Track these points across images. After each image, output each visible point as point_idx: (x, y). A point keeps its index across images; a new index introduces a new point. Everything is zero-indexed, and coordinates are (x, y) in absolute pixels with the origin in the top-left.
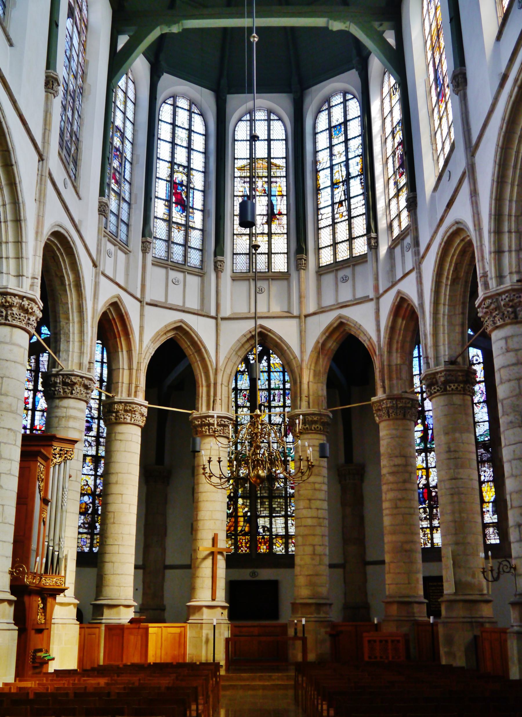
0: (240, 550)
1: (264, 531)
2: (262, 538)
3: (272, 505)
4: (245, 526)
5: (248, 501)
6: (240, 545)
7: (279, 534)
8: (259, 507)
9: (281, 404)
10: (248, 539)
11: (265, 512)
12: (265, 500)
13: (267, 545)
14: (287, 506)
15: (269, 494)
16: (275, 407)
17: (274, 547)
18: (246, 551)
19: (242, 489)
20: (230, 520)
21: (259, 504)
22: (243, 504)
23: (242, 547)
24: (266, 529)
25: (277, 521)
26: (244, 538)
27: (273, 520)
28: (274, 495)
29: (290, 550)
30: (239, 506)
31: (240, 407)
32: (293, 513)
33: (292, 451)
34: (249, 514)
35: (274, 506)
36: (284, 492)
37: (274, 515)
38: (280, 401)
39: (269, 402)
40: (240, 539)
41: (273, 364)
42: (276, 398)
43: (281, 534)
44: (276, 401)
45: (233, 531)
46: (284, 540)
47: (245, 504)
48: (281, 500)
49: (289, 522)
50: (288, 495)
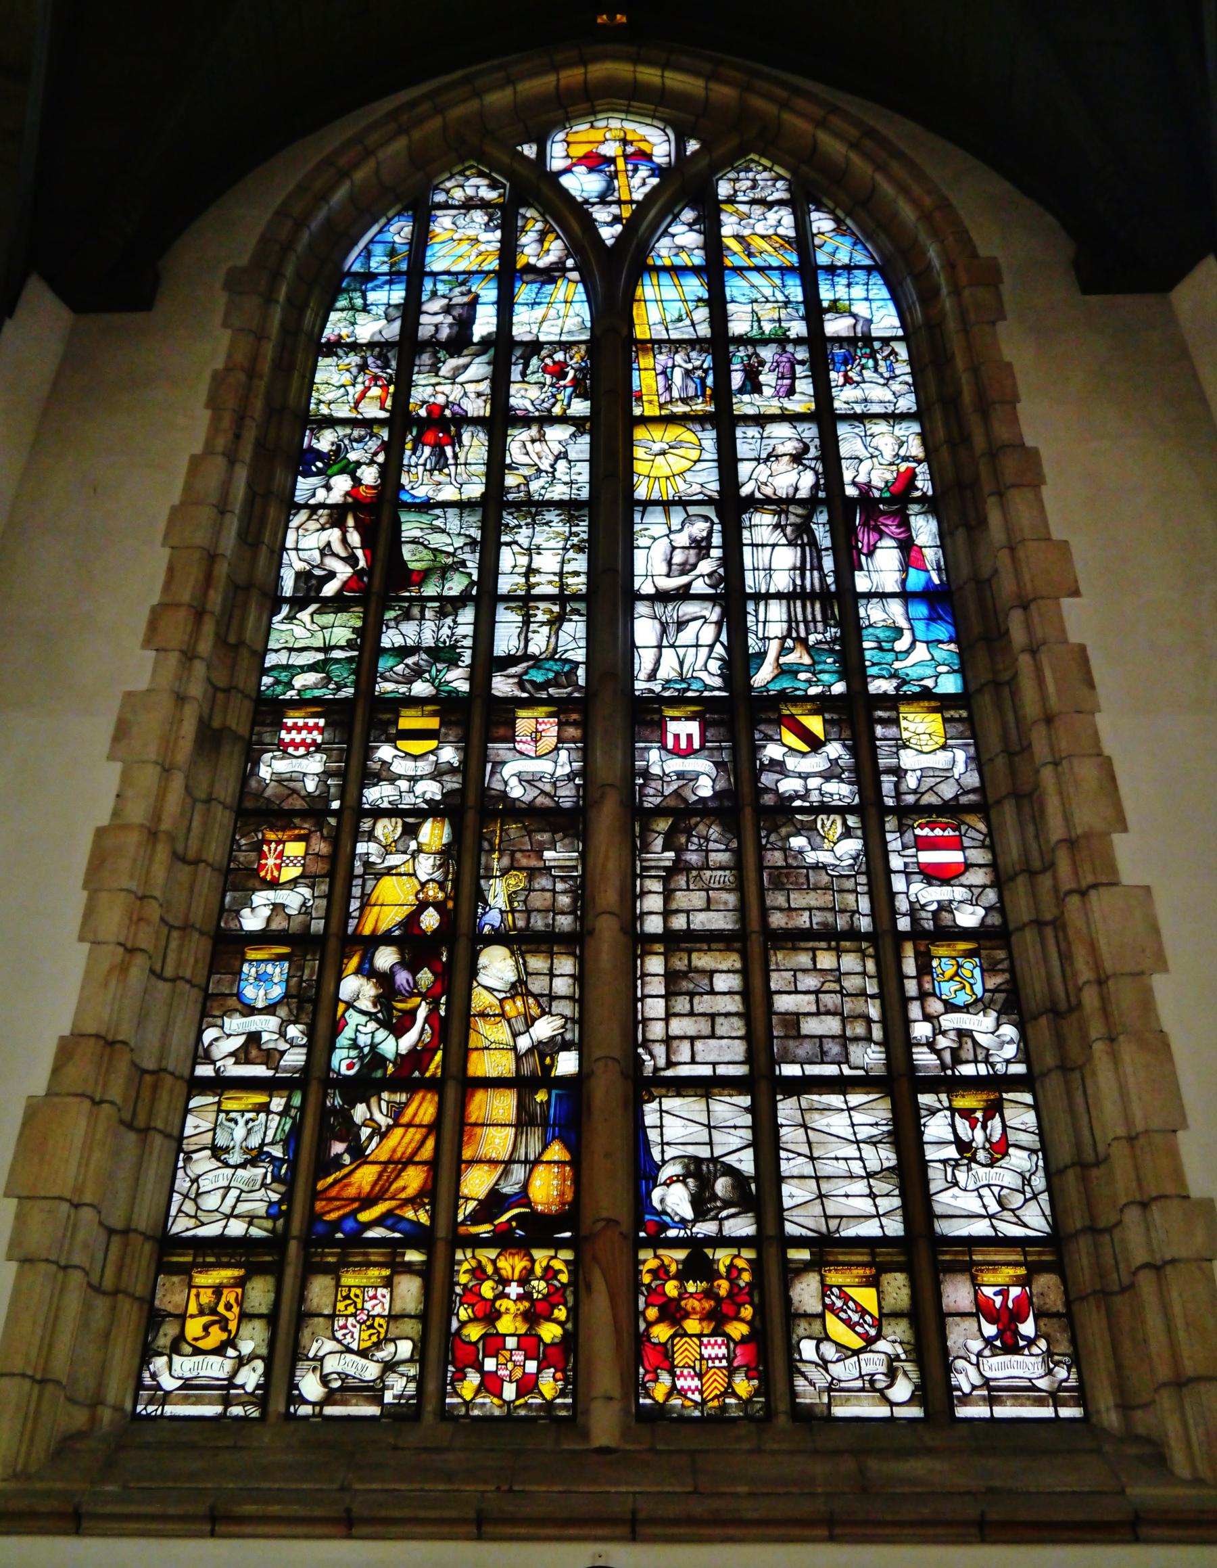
0: (473, 1379)
1: (702, 1204)
2: (688, 1271)
3: (769, 995)
4: (533, 1164)
5: (566, 965)
6: (474, 1333)
7: (850, 1231)
8: (655, 1008)
9: (802, 402)
10: (549, 1273)
11: (708, 1050)
12: (703, 961)
13: (738, 1330)
14: (905, 1001)
15: (742, 910)
16: (761, 420)
17: (808, 1349)
18: (527, 1385)
19: (517, 881)
20: (397, 1112)
21: (657, 986)
22: (518, 988)
23: (494, 1344)
24: (722, 1186)
25: (819, 1121)
26: (512, 1265)
27: (787, 1109)
28: (777, 920)
29: (965, 1378)
30: (481, 1000)
31: (526, 421)
32: (957, 1060)
33: (902, 645)
34: (567, 1063)
35: (783, 1003)
36: (864, 904)
37: (790, 1070)
38: (791, 391)
39: (722, 394)
40: (478, 1273)
41: (739, 238)
42: (767, 377)
43: (870, 1229)
44: (768, 391)
45: (413, 1202)
46: (897, 1287)
47: (536, 985)
48: (850, 962)
49: (936, 1128)
50: (904, 924)
